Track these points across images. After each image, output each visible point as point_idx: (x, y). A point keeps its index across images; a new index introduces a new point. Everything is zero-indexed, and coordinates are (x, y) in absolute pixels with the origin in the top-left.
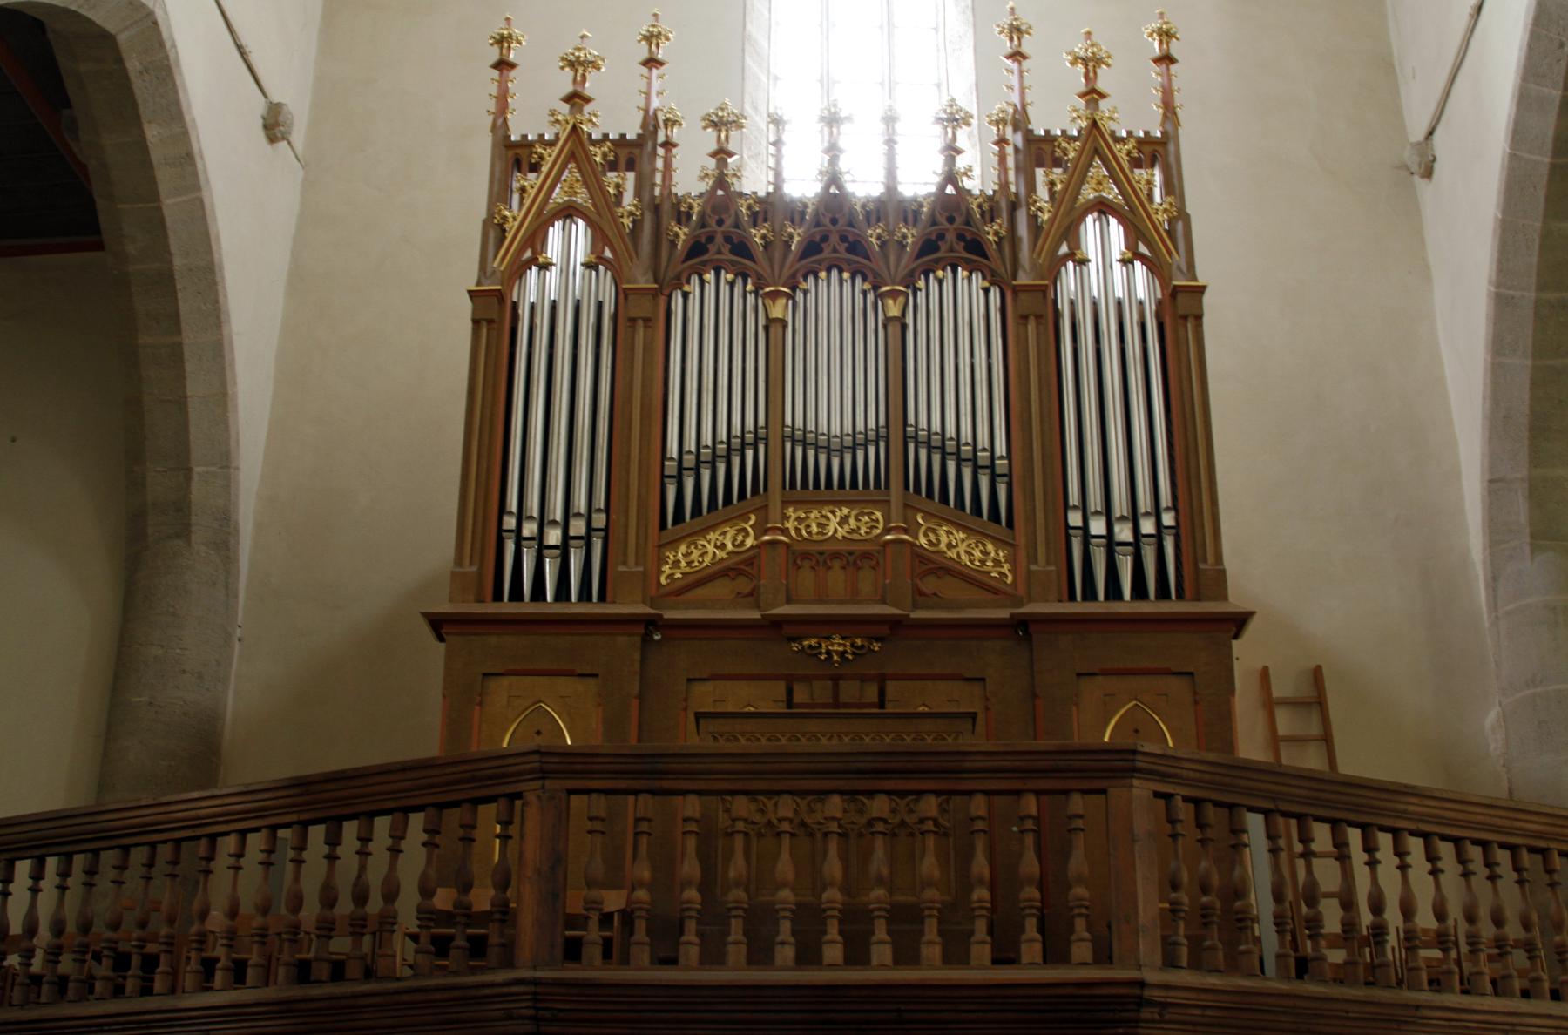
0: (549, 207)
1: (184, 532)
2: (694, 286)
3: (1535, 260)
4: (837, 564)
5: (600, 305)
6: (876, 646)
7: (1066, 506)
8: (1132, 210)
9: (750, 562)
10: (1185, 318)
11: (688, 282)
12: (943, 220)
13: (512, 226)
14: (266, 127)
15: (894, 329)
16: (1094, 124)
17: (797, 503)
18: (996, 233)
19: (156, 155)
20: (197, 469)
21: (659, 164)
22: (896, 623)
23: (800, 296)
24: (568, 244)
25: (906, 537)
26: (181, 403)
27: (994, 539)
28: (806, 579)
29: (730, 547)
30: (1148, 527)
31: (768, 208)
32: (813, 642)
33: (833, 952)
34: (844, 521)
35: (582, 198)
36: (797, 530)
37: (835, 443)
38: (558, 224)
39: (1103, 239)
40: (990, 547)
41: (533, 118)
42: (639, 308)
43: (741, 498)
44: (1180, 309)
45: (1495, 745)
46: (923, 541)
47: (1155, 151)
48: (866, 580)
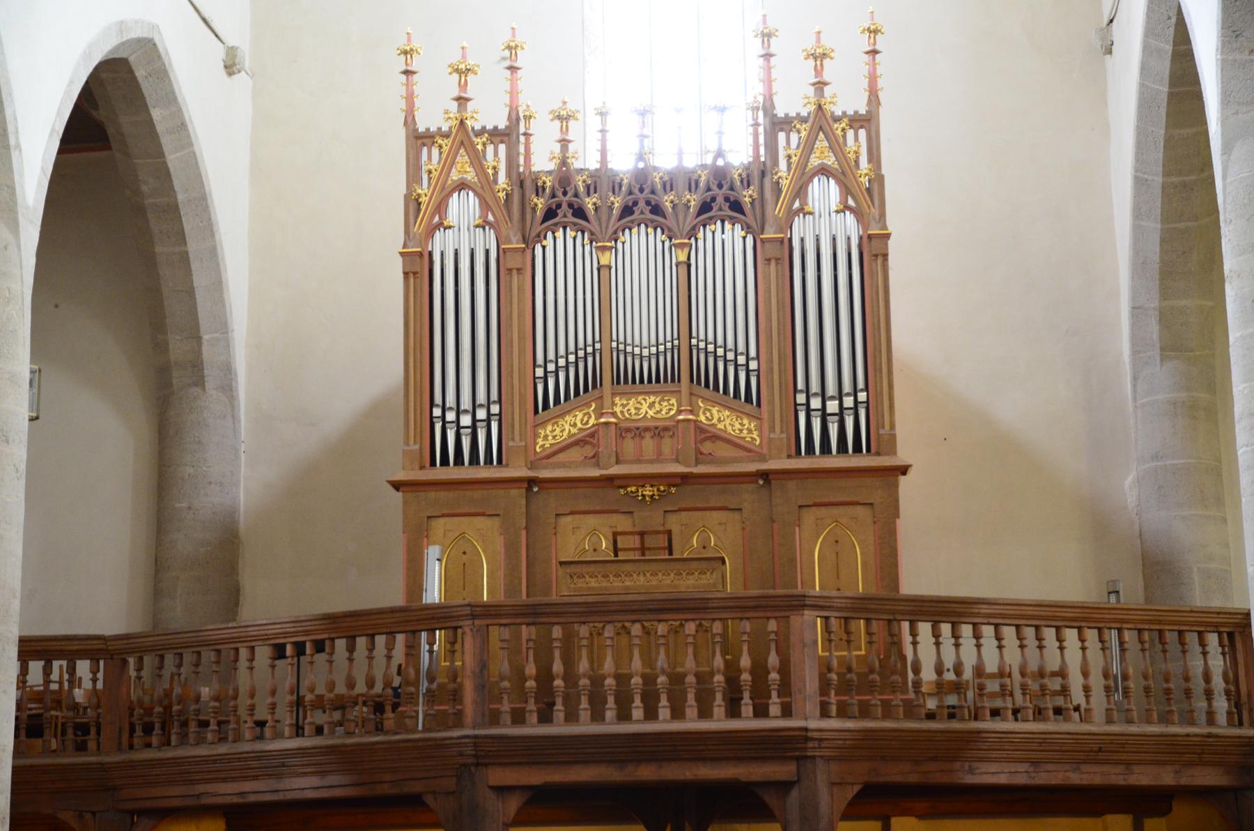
0: (449, 182)
1: (200, 382)
2: (549, 242)
3: (1161, 155)
4: (648, 435)
5: (487, 252)
6: (673, 490)
7: (796, 390)
8: (843, 173)
9: (592, 435)
10: (876, 256)
11: (545, 238)
12: (715, 187)
13: (423, 199)
14: (226, 67)
15: (683, 269)
16: (820, 107)
17: (622, 394)
18: (751, 196)
19: (160, 128)
20: (205, 337)
21: (522, 149)
22: (685, 478)
23: (620, 245)
24: (463, 208)
25: (691, 417)
26: (191, 292)
27: (748, 415)
28: (629, 445)
29: (579, 425)
30: (849, 402)
31: (599, 181)
32: (634, 489)
33: (638, 713)
34: (652, 405)
35: (471, 176)
36: (622, 412)
37: (645, 352)
38: (455, 195)
39: (824, 194)
40: (745, 421)
41: (432, 117)
42: (512, 262)
43: (586, 388)
44: (874, 250)
45: (1131, 498)
46: (702, 418)
47: (866, 121)
48: (667, 445)
